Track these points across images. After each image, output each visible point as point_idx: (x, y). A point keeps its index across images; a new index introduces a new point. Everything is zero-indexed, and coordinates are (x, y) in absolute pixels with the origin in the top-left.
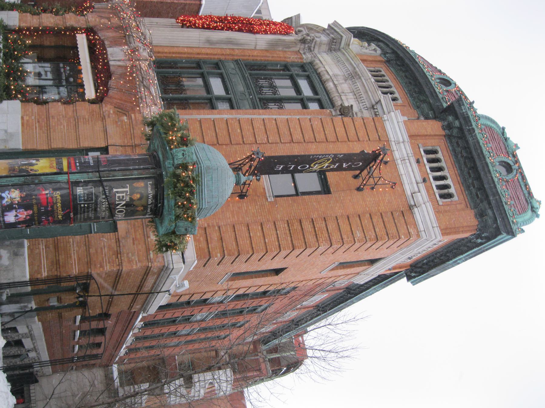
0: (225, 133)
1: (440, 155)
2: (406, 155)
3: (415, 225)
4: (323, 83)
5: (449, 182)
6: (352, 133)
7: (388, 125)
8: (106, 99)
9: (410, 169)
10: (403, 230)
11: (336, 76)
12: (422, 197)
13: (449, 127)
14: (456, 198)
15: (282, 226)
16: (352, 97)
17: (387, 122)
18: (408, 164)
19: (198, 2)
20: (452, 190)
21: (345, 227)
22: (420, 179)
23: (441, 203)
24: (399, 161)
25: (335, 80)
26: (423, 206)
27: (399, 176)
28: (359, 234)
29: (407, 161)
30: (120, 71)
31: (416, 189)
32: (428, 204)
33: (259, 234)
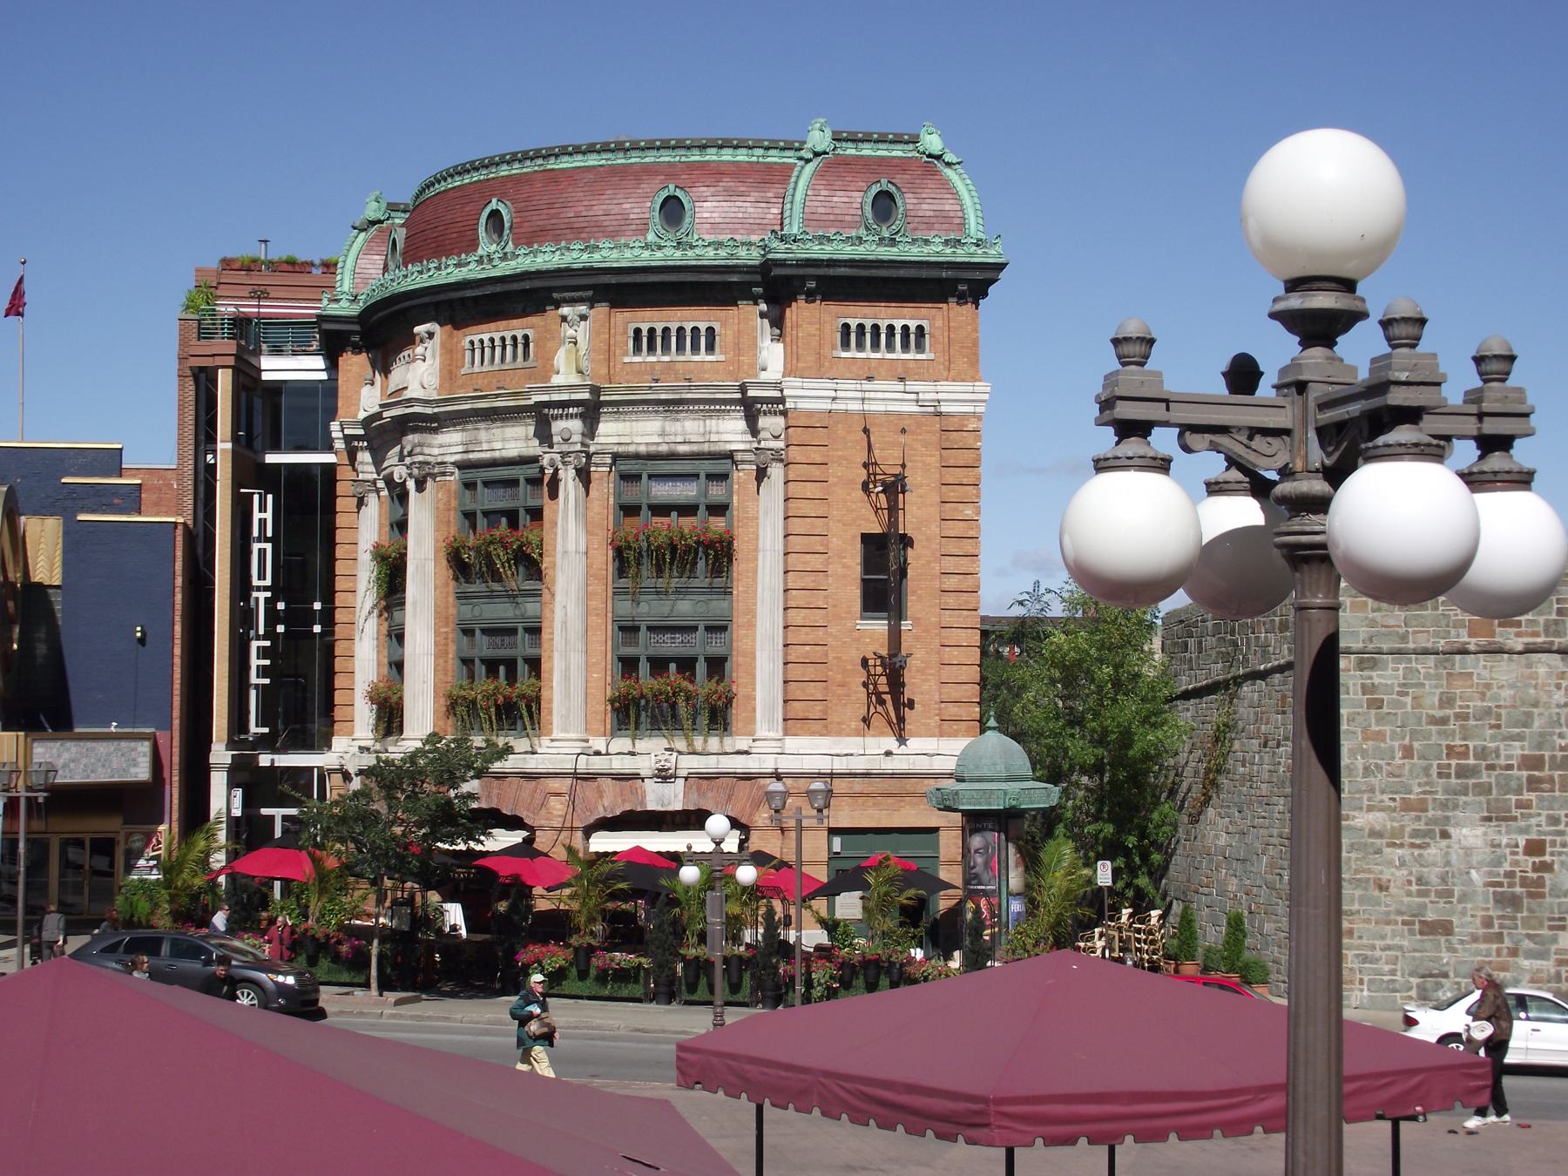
0: (811, 668)
1: (853, 323)
2: (859, 395)
3: (964, 415)
4: (672, 456)
5: (898, 324)
6: (815, 472)
7: (804, 405)
8: (743, 821)
9: (880, 395)
10: (969, 440)
11: (663, 434)
12: (927, 390)
13: (811, 297)
14: (925, 323)
15: (948, 619)
16: (714, 422)
17: (799, 406)
18: (872, 395)
19: (180, 527)
20: (913, 325)
21: (956, 529)
22: (900, 387)
23: (932, 356)
24: (866, 407)
25: (672, 439)
26: (940, 396)
27: (887, 413)
28: (968, 512)
29: (867, 395)
30: (694, 796)
31: (913, 396)
32: (939, 388)
33: (955, 651)
